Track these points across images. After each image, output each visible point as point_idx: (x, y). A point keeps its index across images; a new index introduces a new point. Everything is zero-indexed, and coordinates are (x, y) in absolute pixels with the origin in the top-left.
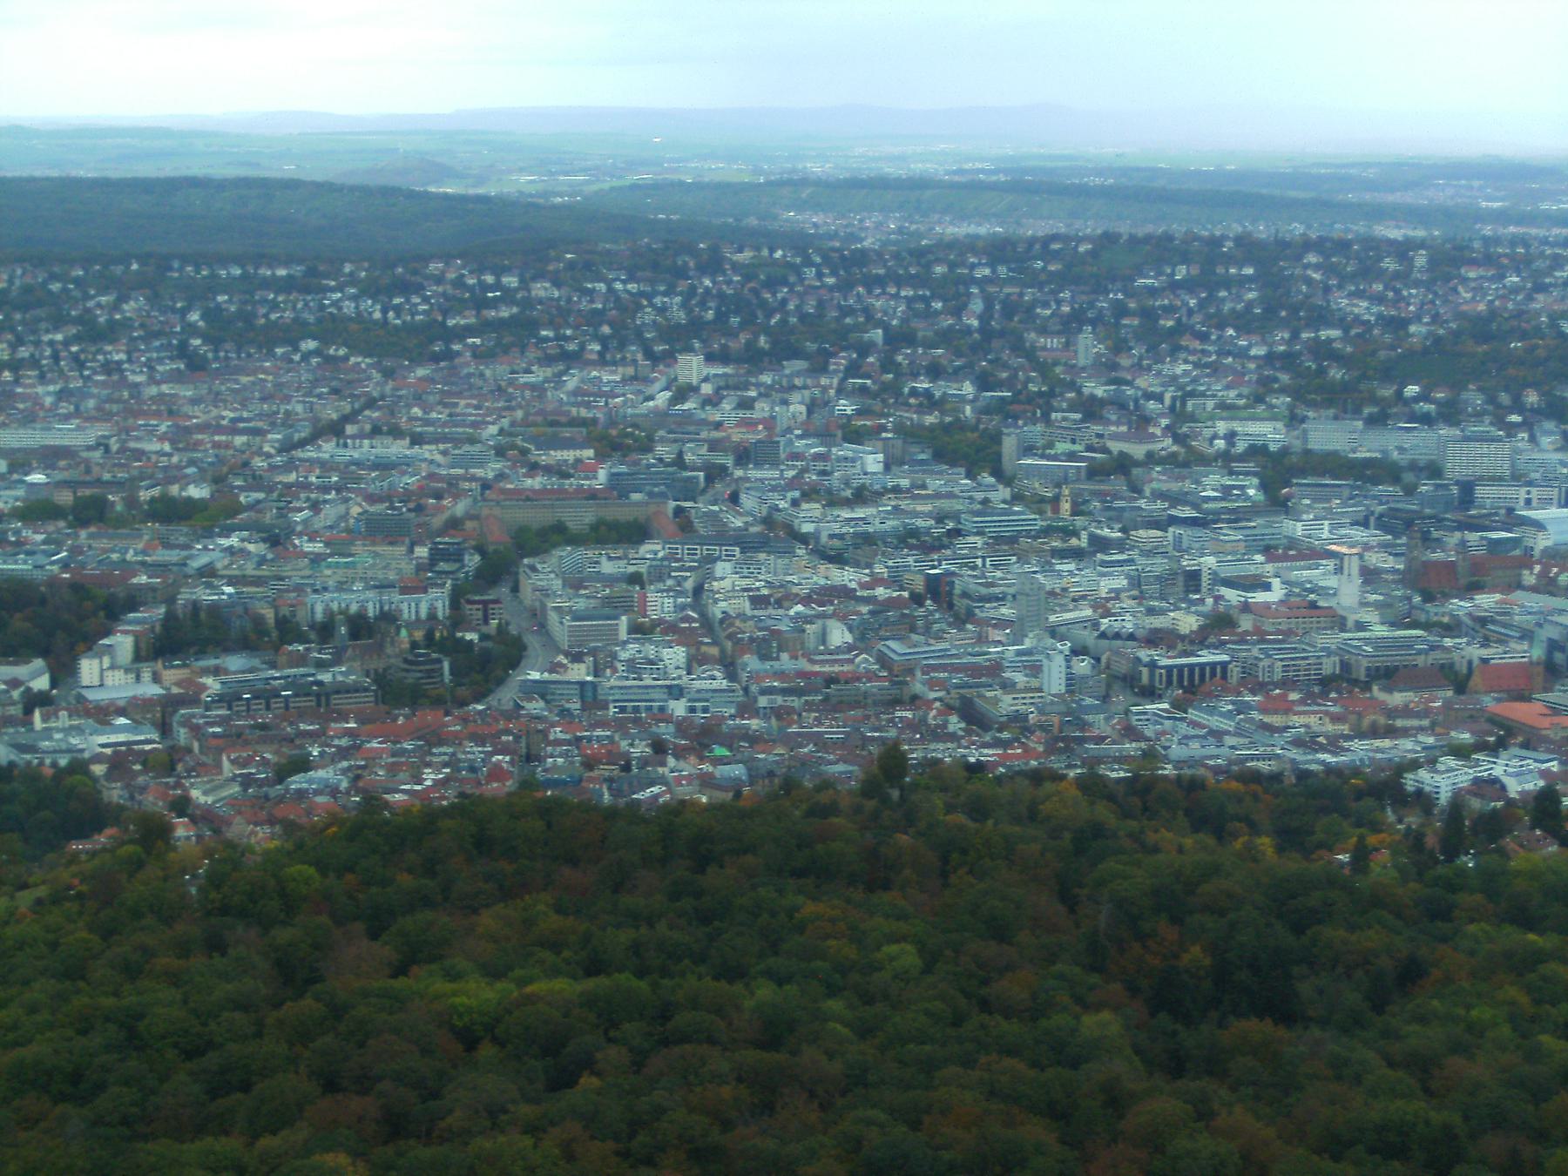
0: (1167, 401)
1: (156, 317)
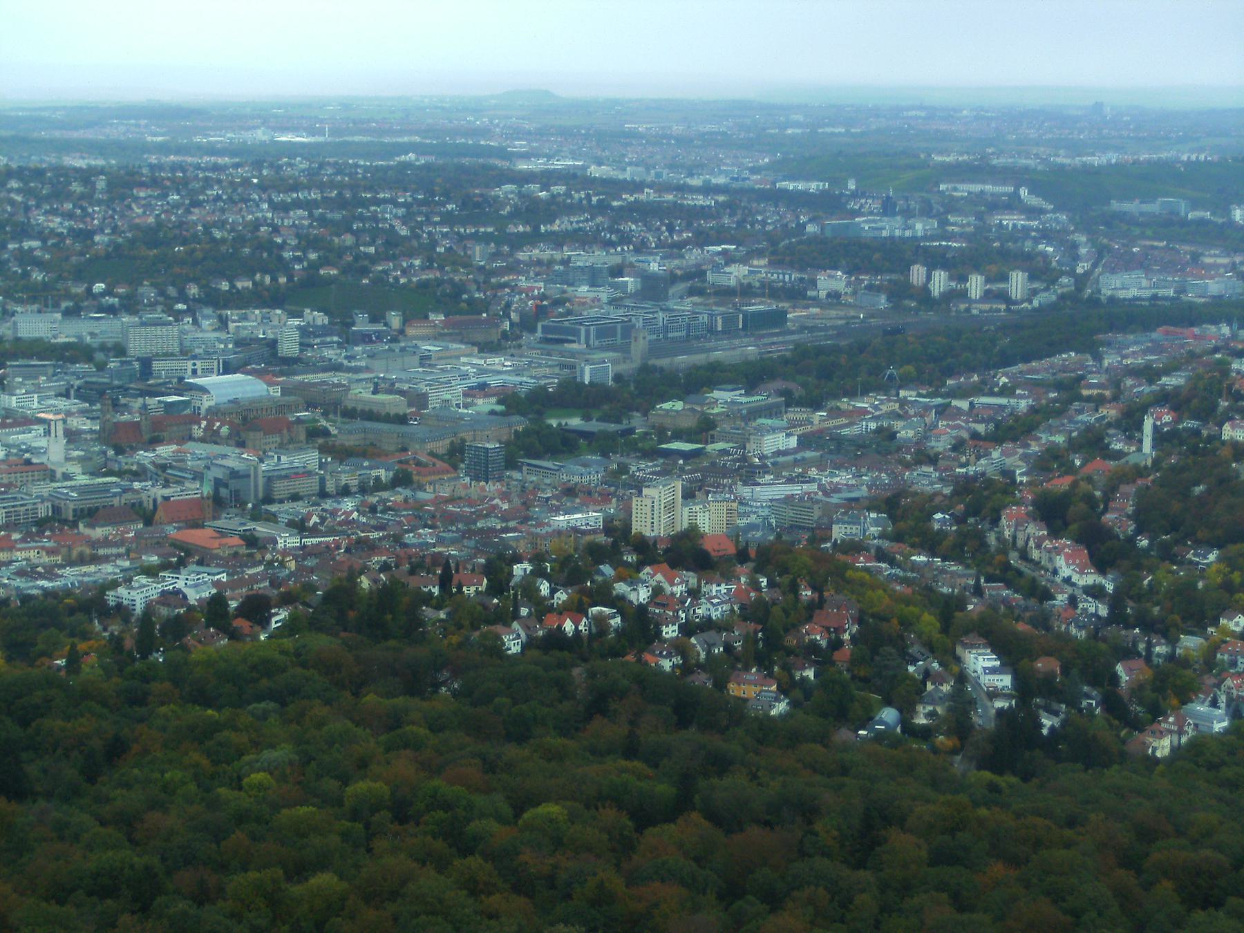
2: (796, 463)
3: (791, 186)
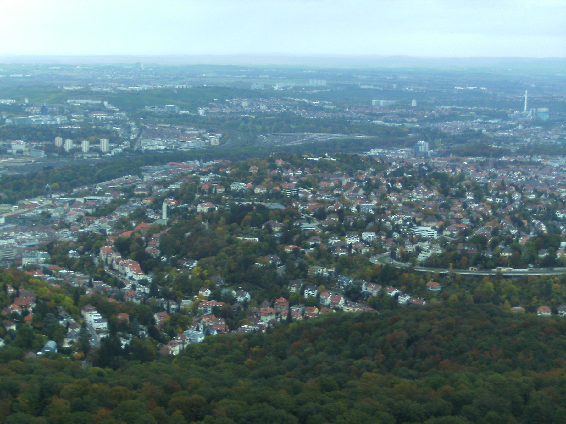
2: (5, 230)
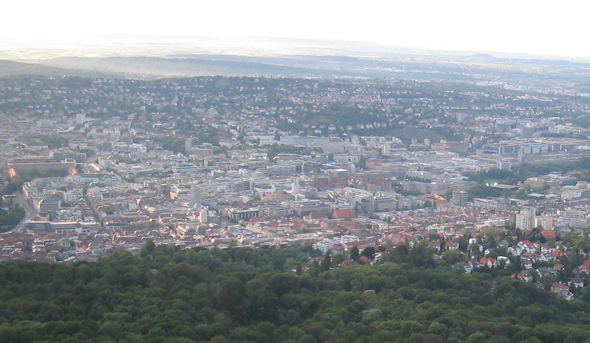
0: (275, 131)
1: (204, 127)
2: (580, 203)
3: (582, 95)
